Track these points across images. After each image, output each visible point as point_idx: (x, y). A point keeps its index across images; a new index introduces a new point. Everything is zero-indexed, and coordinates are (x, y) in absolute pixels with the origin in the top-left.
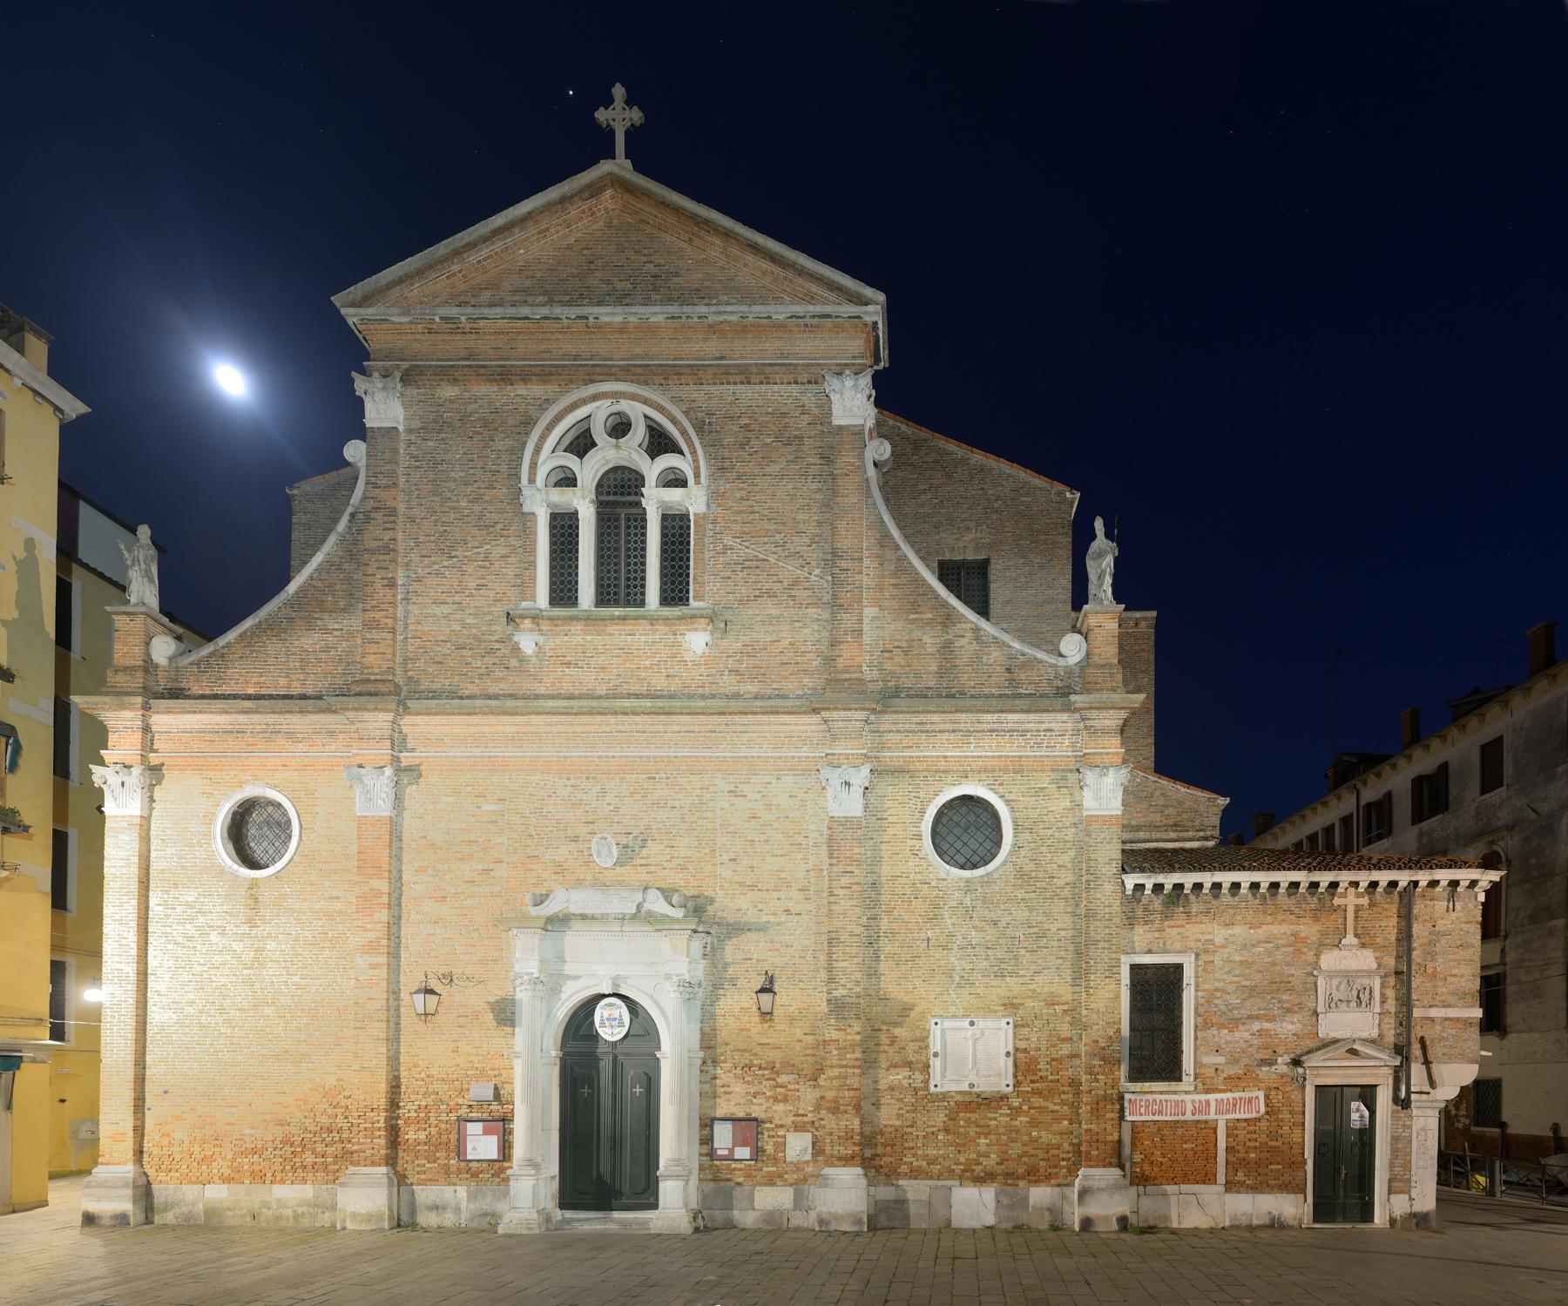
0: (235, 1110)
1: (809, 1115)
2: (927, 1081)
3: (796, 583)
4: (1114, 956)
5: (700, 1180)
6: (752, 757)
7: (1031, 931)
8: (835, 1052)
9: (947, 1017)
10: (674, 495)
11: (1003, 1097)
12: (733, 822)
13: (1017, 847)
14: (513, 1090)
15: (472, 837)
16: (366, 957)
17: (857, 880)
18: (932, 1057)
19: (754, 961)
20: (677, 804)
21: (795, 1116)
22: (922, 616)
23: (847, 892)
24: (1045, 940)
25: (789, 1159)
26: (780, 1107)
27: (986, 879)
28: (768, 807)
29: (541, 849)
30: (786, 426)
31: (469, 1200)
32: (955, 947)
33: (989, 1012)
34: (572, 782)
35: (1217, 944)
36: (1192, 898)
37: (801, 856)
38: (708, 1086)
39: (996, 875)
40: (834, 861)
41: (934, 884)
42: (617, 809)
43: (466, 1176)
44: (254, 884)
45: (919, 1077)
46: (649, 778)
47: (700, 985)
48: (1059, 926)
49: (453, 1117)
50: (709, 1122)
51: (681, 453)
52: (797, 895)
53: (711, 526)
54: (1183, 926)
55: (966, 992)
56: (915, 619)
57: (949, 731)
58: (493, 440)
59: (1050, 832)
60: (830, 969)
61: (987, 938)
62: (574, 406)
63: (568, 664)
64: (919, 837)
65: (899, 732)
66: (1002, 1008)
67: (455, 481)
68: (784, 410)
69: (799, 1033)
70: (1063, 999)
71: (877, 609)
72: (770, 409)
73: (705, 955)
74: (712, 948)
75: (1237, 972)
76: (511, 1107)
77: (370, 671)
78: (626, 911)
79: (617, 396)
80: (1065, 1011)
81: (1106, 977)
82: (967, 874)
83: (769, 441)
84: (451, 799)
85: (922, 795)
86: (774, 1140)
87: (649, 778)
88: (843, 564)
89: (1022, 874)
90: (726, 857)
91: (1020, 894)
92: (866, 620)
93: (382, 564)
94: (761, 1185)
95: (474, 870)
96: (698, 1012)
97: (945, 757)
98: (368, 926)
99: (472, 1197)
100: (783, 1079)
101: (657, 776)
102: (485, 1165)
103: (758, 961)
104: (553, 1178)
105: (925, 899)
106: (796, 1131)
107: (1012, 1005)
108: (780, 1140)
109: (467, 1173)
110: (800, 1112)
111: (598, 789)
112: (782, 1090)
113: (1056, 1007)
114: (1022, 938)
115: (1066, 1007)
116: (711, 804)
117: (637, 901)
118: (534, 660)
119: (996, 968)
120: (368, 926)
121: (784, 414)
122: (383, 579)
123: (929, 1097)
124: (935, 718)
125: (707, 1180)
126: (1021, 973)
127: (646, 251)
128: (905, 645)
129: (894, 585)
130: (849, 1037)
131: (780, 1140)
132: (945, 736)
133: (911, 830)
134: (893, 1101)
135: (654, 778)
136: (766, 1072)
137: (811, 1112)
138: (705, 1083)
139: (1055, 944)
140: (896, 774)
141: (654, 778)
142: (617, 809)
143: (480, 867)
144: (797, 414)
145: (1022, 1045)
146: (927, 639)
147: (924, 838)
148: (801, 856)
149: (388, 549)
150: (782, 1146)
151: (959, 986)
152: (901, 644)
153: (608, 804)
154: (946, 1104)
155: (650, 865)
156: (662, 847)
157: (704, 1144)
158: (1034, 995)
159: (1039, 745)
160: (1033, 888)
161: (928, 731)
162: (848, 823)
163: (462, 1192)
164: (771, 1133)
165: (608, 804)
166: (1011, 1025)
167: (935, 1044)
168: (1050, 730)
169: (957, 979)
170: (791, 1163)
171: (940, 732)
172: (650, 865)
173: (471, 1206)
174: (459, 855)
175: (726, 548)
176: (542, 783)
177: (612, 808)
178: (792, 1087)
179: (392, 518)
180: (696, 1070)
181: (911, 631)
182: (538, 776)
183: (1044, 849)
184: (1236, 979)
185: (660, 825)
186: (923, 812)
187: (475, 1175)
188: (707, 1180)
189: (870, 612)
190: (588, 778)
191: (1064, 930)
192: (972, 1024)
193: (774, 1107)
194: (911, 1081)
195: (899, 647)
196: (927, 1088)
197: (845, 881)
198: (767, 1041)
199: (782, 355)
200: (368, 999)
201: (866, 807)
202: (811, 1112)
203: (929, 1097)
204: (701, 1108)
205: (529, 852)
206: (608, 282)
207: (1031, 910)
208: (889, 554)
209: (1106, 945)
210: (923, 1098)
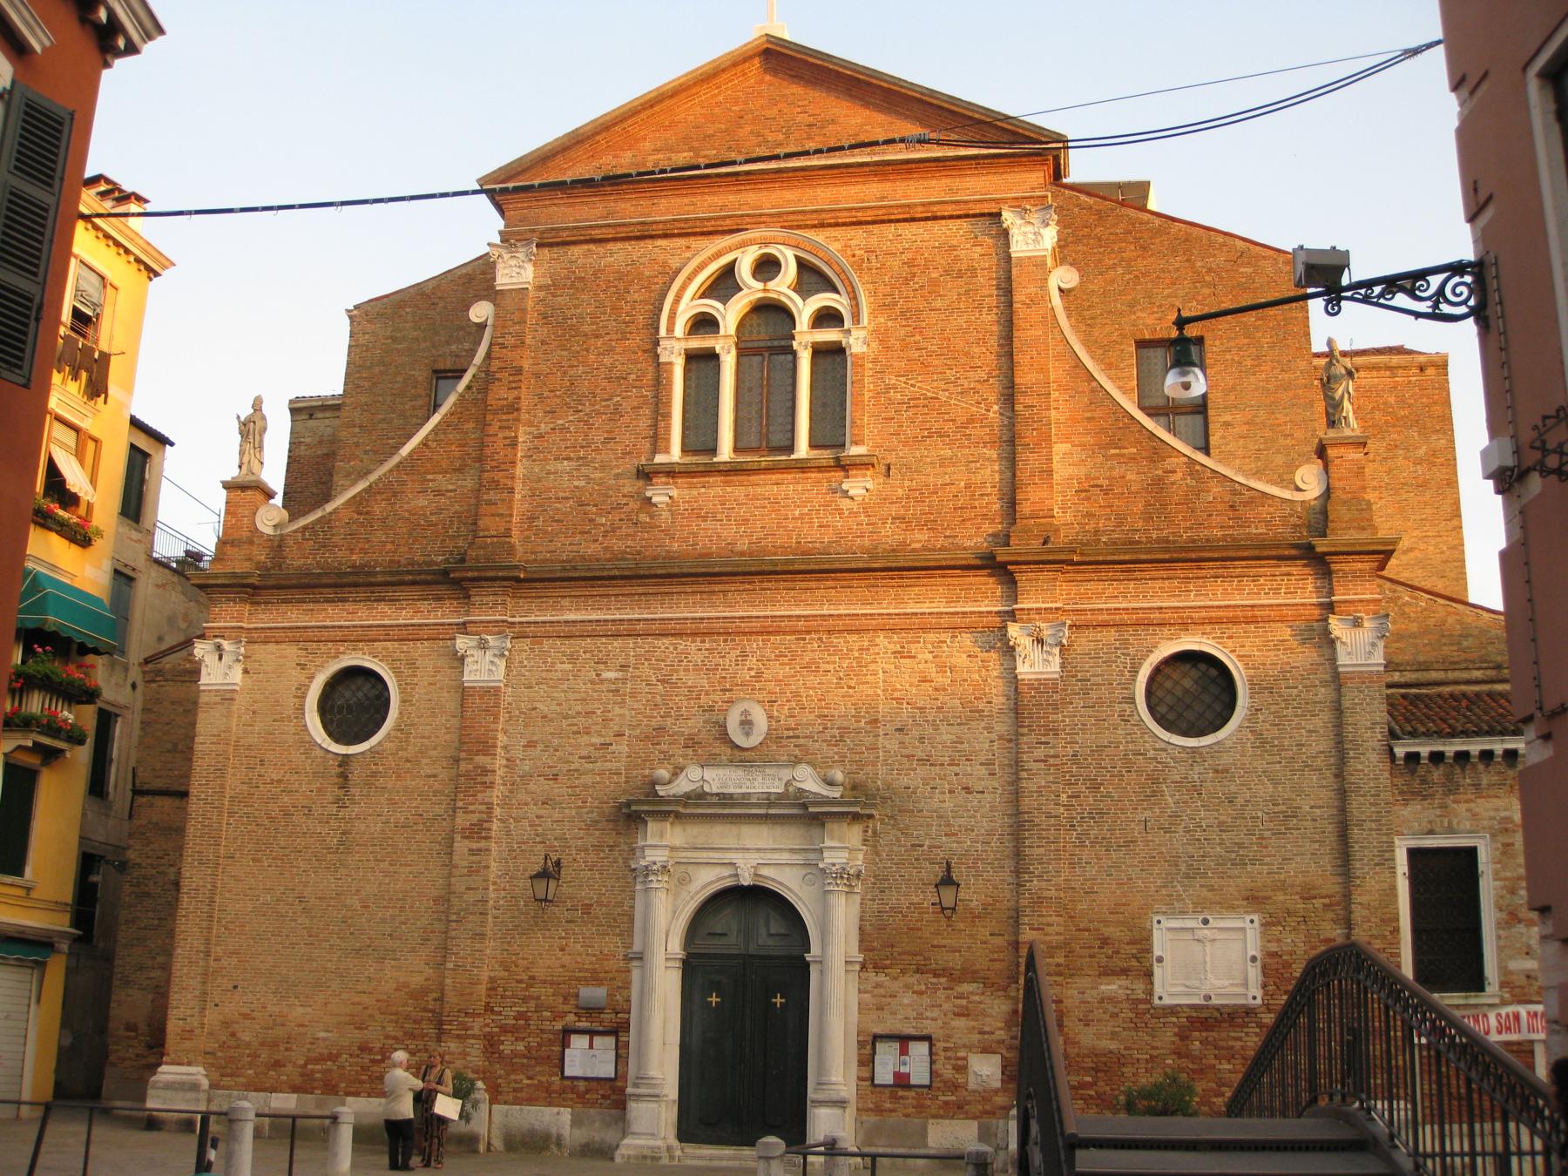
0: (309, 1010)
1: (998, 1032)
2: (1150, 993)
3: (971, 421)
4: (1385, 839)
5: (858, 1109)
6: (924, 614)
7: (1277, 809)
9: (1173, 914)
10: (829, 335)
11: (1248, 1011)
12: (899, 687)
13: (1255, 711)
14: (629, 996)
15: (589, 708)
16: (466, 841)
17: (1052, 752)
18: (1155, 964)
19: (925, 847)
20: (830, 667)
21: (980, 1033)
22: (1123, 451)
23: (1042, 765)
24: (1295, 821)
25: (972, 1086)
26: (960, 1023)
27: (1216, 748)
28: (941, 668)
29: (669, 721)
30: (957, 259)
31: (572, 1127)
32: (1180, 829)
33: (1227, 906)
34: (707, 645)
36: (1481, 767)
37: (983, 724)
38: (866, 995)
39: (1229, 744)
40: (1025, 730)
41: (1151, 754)
42: (759, 675)
43: (570, 1096)
44: (345, 760)
45: (1139, 987)
46: (797, 639)
47: (858, 876)
48: (1312, 803)
49: (559, 1026)
50: (870, 1039)
51: (836, 291)
52: (983, 771)
53: (870, 365)
54: (1472, 801)
56: (1117, 455)
57: (1163, 579)
58: (628, 292)
59: (1295, 691)
60: (1018, 854)
61: (1222, 818)
62: (718, 255)
63: (705, 518)
64: (1131, 700)
66: (1245, 903)
67: (586, 335)
68: (955, 242)
69: (983, 932)
70: (1324, 892)
71: (1069, 445)
72: (937, 244)
73: (865, 840)
74: (875, 832)
76: (626, 1016)
77: (486, 533)
78: (773, 791)
79: (766, 243)
80: (1325, 905)
81: (1377, 864)
82: (1192, 742)
83: (935, 275)
84: (568, 667)
85: (1131, 651)
86: (953, 1062)
87: (797, 639)
88: (1028, 401)
89: (1262, 743)
90: (890, 728)
91: (1260, 765)
92: (1056, 458)
93: (504, 424)
94: (935, 1117)
95: (592, 745)
96: (857, 906)
98: (471, 808)
99: (576, 1122)
101: (808, 637)
102: (594, 1084)
103: (930, 847)
104: (674, 1101)
105: (1139, 772)
107: (1255, 899)
108: (960, 1063)
109: (572, 1093)
110: (987, 1029)
111: (738, 652)
112: (964, 1002)
113: (1314, 901)
114: (1266, 817)
115: (1327, 901)
116: (872, 667)
117: (785, 779)
118: (665, 515)
119: (1233, 856)
120: (471, 808)
121: (954, 248)
122: (505, 438)
123: (1152, 1011)
125: (867, 1110)
126: (1267, 860)
127: (800, 103)
128: (1105, 483)
129: (1088, 418)
130: (1048, 938)
131: (960, 1063)
133: (1119, 693)
134: (1106, 1017)
135: (805, 639)
136: (943, 980)
138: (867, 992)
139: (1308, 824)
140: (1099, 629)
141: (805, 639)
142: (759, 675)
143: (597, 740)
144: (968, 246)
145: (1273, 947)
146: (1130, 476)
148: (983, 724)
149: (513, 408)
150: (962, 1068)
151: (1187, 876)
152: (1099, 482)
153: (749, 669)
154: (1175, 1020)
155: (798, 737)
156: (812, 717)
157: (864, 1066)
158: (1282, 887)
159: (1276, 591)
162: (1043, 686)
163: (566, 1114)
164: (949, 1054)
165: (749, 669)
166: (1256, 924)
167: (1161, 943)
168: (1289, 574)
169: (1183, 868)
170: (975, 1091)
172: (798, 737)
173: (577, 1132)
174: (575, 728)
175: (888, 388)
176: (671, 649)
177: (753, 673)
178: (977, 998)
179: (517, 378)
181: (1112, 468)
182: (666, 641)
185: (811, 692)
186: (1135, 671)
187: (581, 1096)
188: (867, 1110)
189: (1060, 449)
190: (725, 641)
191: (1319, 807)
193: (953, 1023)
194: (1129, 992)
195: (1097, 486)
196: (1149, 1001)
197: (1040, 752)
198: (944, 942)
199: (951, 191)
200: (468, 889)
201: (1063, 666)
202: (1000, 1029)
203: (1152, 1011)
204: (859, 1022)
205: (654, 723)
206: (759, 135)
207: (1275, 783)
208: (1084, 386)
209: (1373, 825)
210: (1145, 1012)
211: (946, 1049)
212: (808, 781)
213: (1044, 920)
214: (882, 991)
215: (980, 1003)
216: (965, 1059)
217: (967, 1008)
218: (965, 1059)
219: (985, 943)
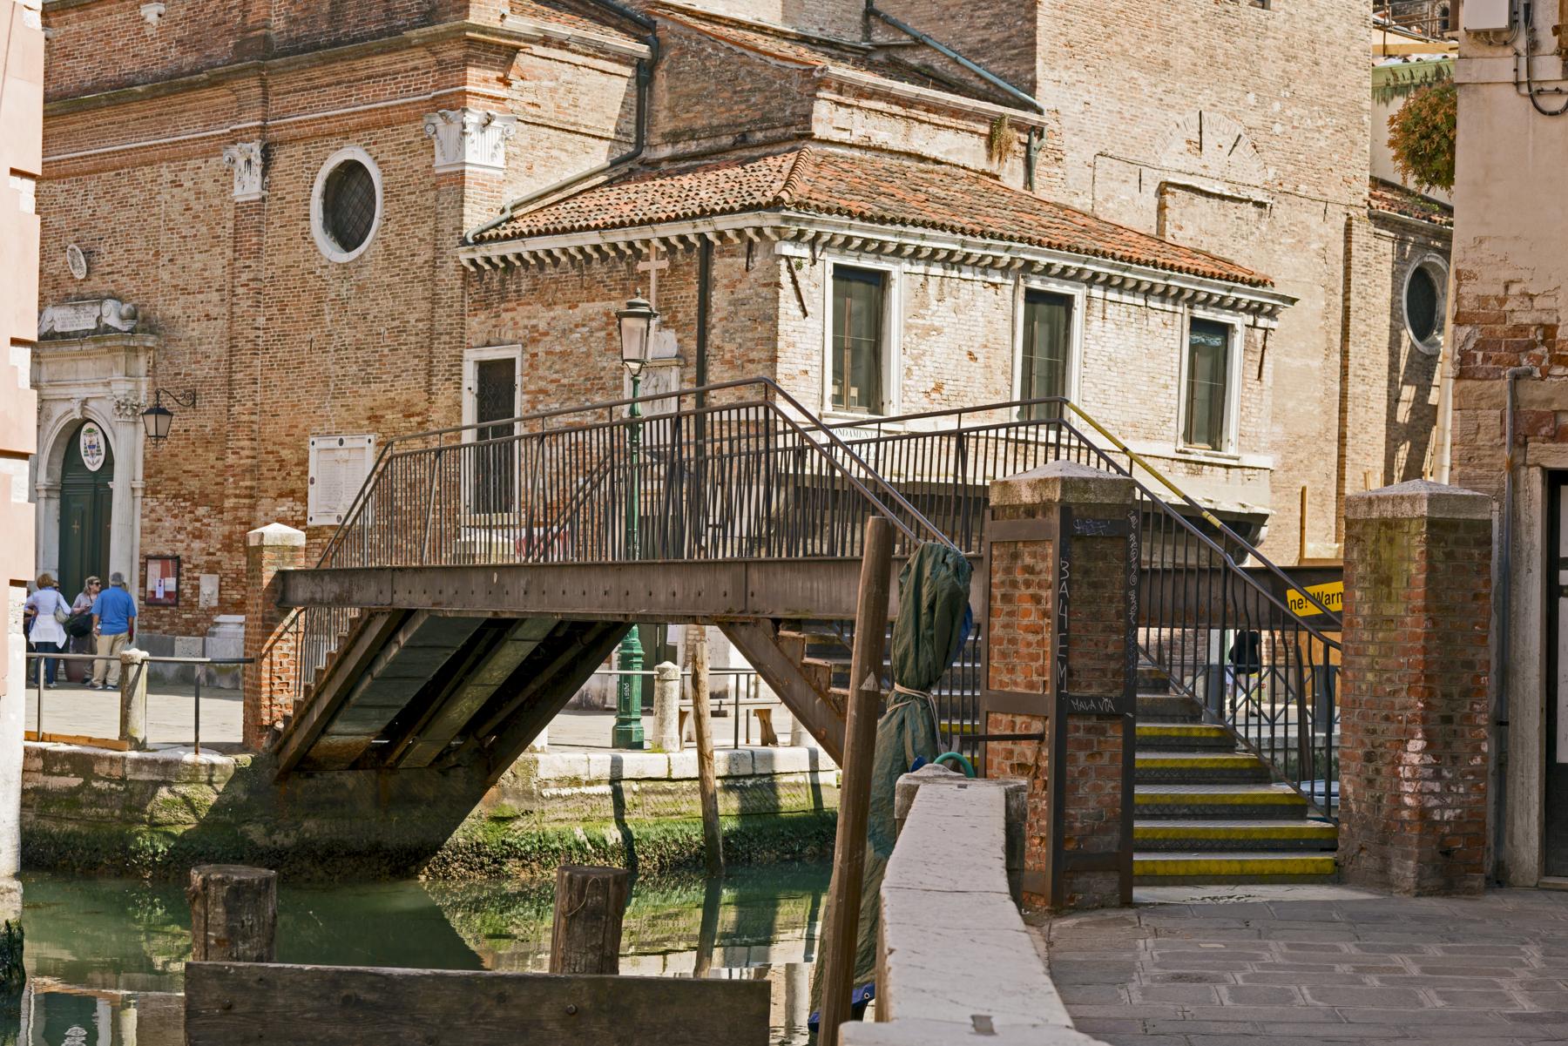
8: (231, 480)
26: (197, 545)
35: (541, 330)
41: (318, 273)
52: (215, 297)
54: (513, 310)
55: (338, 403)
61: (359, 336)
65: (296, 91)
75: (557, 367)
97: (327, 118)
100: (201, 511)
103: (186, 375)
106: (208, 573)
108: (195, 582)
112: (198, 524)
124: (318, 73)
130: (242, 462)
131: (195, 582)
132: (332, 90)
136: (188, 504)
137: (219, 550)
147: (311, 217)
160: (397, 270)
161: (316, 87)
171: (327, 86)
180: (138, 502)
183: (407, 220)
184: (556, 376)
192: (341, 442)
197: (244, 277)
202: (219, 550)
211: (189, 570)
212: (112, 314)
213: (242, 444)
214: (153, 516)
215: (209, 525)
216: (198, 579)
217: (201, 531)
218: (198, 579)
219: (213, 467)
